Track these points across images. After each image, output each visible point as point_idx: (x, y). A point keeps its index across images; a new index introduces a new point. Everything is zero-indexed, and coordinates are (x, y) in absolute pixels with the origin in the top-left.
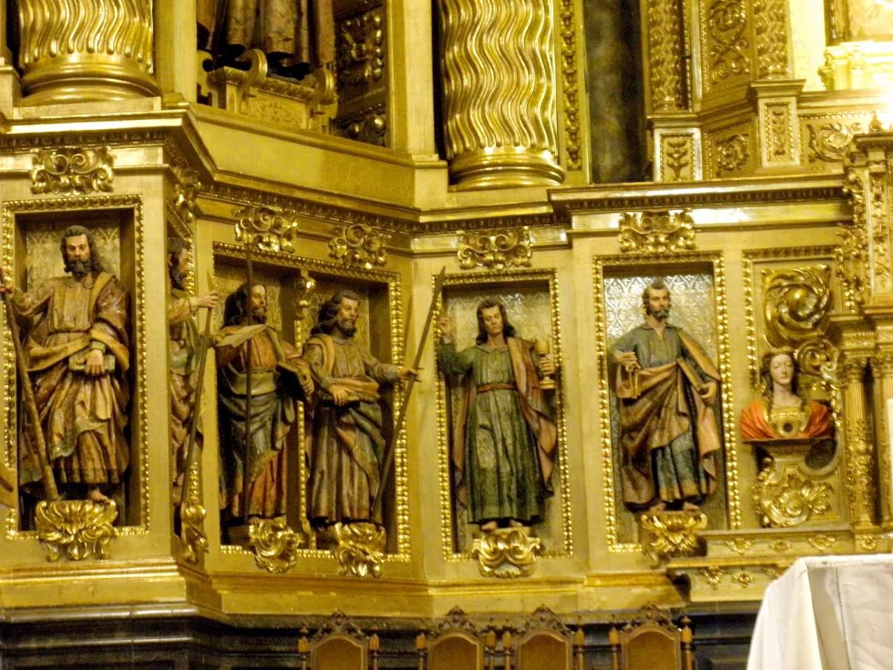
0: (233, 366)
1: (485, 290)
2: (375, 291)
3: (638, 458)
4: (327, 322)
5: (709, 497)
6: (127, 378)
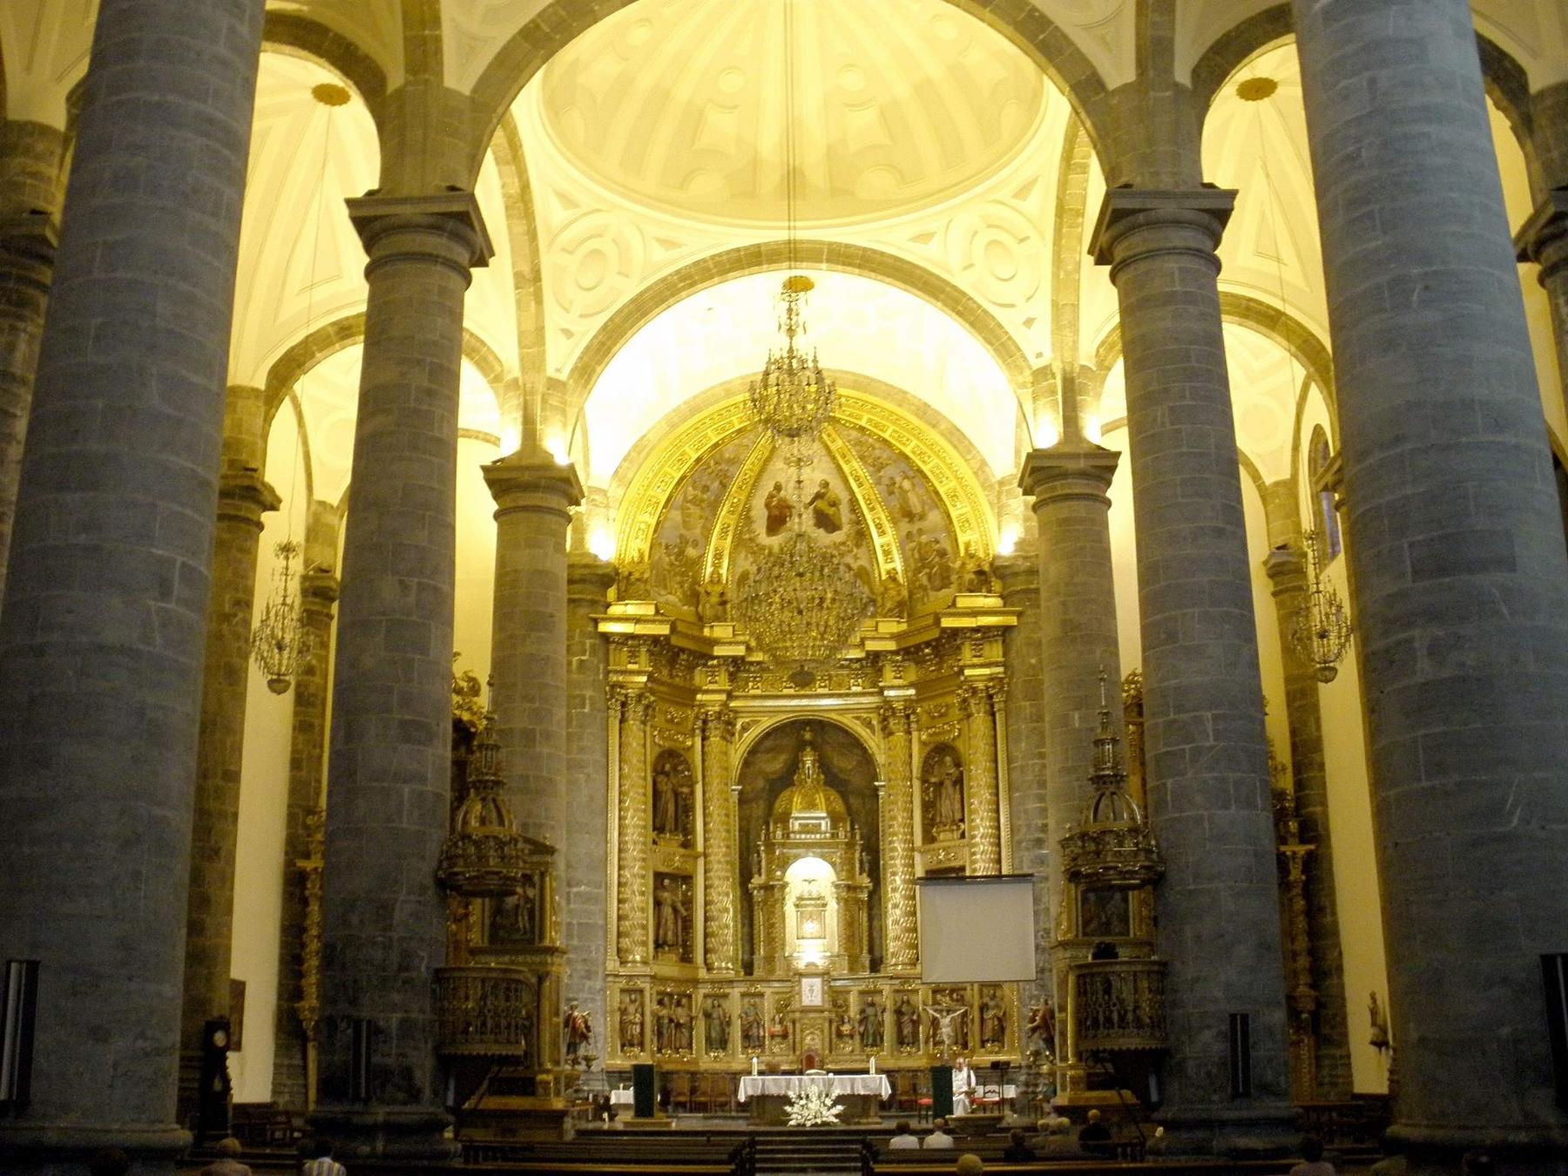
0: (659, 1019)
1: (716, 996)
2: (690, 996)
3: (746, 1037)
4: (679, 1004)
5: (762, 1046)
6: (642, 1024)
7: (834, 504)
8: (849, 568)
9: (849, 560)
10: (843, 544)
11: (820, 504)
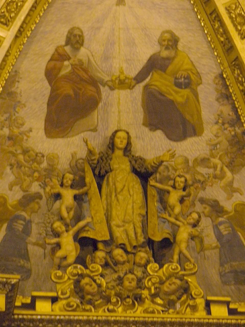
7: (187, 83)
8: (216, 209)
9: (215, 192)
10: (204, 161)
11: (160, 81)
